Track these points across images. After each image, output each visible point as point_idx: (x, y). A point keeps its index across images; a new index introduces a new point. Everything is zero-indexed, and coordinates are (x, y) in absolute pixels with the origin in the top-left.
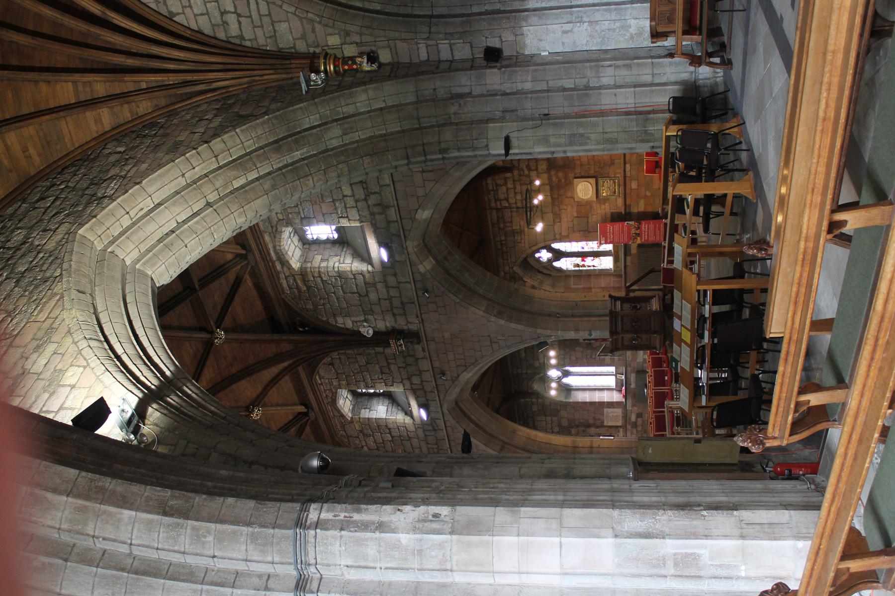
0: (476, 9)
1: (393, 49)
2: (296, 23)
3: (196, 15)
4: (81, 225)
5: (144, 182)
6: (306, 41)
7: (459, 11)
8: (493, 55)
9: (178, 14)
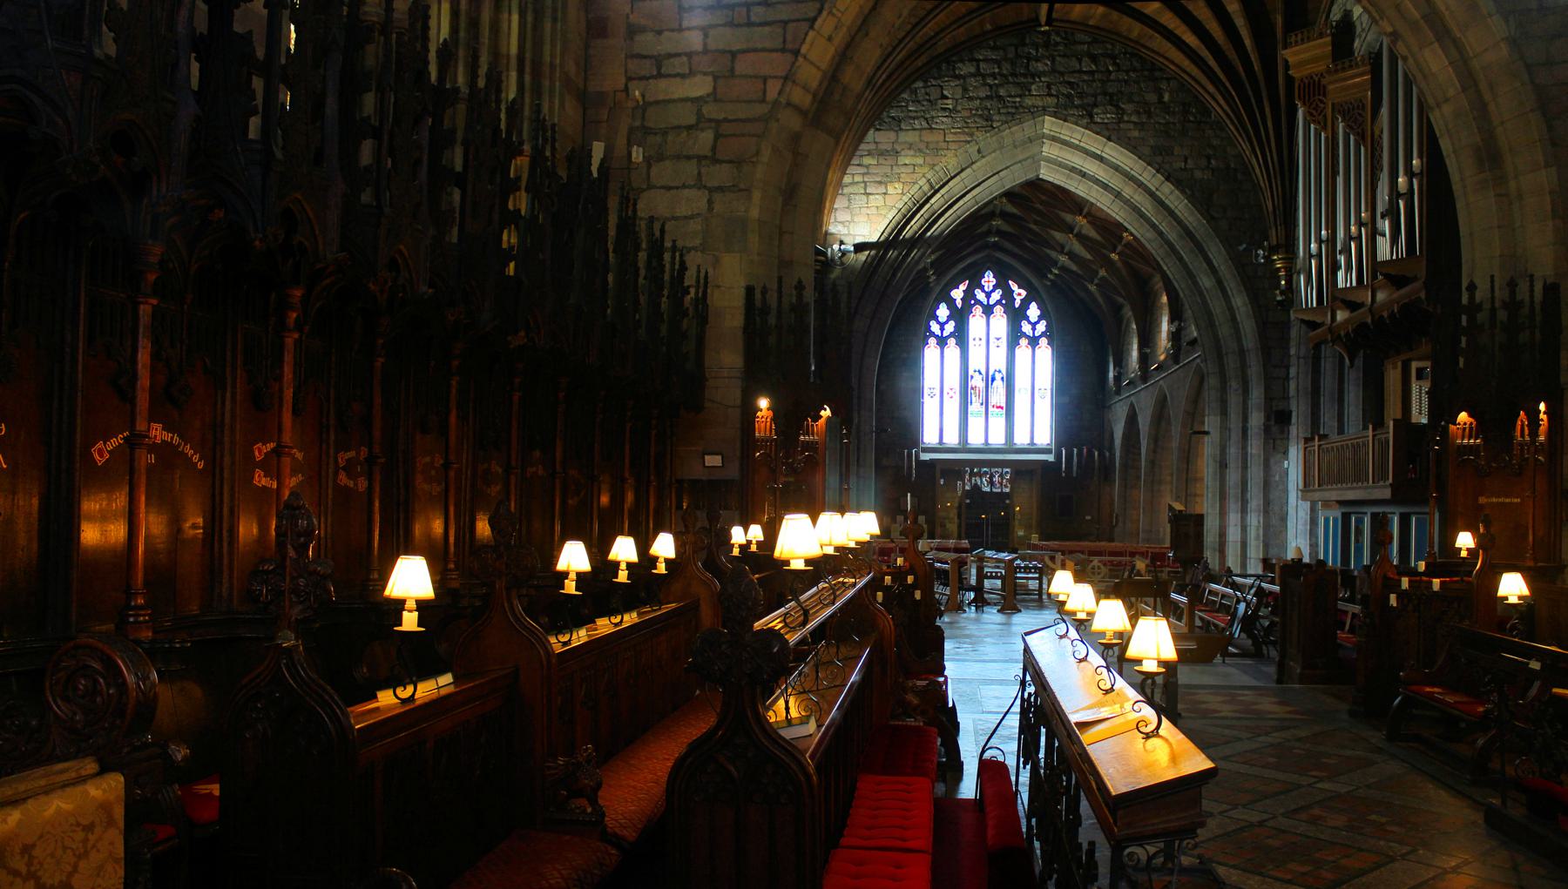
4: (1055, 115)
5: (1111, 143)
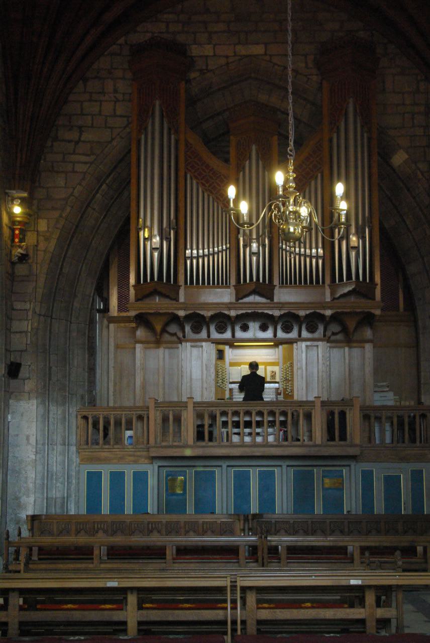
8: (14, 370)
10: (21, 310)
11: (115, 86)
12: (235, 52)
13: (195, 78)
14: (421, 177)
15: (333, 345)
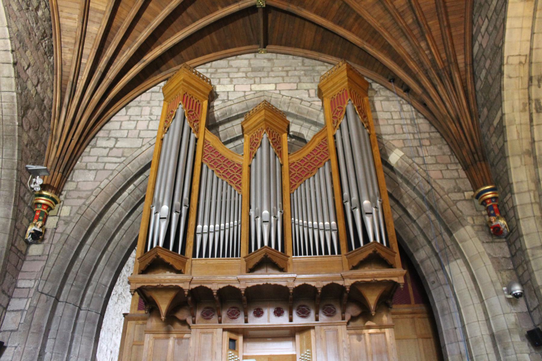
0: (50, 343)
1: (39, 258)
2: (90, 186)
3: (122, 122)
6: (73, 190)
7: (54, 327)
9: (127, 112)
10: (24, 288)
11: (151, 111)
12: (251, 89)
13: (217, 105)
14: (418, 168)
15: (352, 331)
